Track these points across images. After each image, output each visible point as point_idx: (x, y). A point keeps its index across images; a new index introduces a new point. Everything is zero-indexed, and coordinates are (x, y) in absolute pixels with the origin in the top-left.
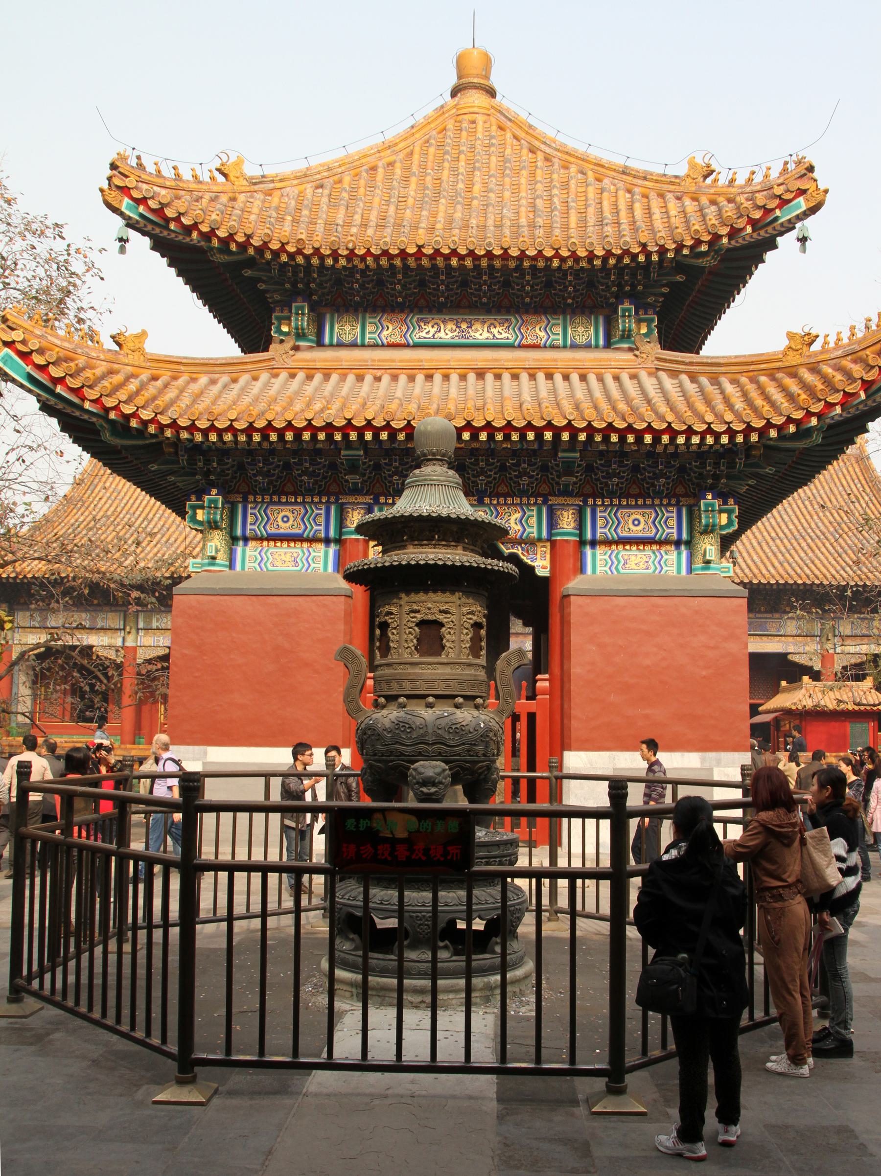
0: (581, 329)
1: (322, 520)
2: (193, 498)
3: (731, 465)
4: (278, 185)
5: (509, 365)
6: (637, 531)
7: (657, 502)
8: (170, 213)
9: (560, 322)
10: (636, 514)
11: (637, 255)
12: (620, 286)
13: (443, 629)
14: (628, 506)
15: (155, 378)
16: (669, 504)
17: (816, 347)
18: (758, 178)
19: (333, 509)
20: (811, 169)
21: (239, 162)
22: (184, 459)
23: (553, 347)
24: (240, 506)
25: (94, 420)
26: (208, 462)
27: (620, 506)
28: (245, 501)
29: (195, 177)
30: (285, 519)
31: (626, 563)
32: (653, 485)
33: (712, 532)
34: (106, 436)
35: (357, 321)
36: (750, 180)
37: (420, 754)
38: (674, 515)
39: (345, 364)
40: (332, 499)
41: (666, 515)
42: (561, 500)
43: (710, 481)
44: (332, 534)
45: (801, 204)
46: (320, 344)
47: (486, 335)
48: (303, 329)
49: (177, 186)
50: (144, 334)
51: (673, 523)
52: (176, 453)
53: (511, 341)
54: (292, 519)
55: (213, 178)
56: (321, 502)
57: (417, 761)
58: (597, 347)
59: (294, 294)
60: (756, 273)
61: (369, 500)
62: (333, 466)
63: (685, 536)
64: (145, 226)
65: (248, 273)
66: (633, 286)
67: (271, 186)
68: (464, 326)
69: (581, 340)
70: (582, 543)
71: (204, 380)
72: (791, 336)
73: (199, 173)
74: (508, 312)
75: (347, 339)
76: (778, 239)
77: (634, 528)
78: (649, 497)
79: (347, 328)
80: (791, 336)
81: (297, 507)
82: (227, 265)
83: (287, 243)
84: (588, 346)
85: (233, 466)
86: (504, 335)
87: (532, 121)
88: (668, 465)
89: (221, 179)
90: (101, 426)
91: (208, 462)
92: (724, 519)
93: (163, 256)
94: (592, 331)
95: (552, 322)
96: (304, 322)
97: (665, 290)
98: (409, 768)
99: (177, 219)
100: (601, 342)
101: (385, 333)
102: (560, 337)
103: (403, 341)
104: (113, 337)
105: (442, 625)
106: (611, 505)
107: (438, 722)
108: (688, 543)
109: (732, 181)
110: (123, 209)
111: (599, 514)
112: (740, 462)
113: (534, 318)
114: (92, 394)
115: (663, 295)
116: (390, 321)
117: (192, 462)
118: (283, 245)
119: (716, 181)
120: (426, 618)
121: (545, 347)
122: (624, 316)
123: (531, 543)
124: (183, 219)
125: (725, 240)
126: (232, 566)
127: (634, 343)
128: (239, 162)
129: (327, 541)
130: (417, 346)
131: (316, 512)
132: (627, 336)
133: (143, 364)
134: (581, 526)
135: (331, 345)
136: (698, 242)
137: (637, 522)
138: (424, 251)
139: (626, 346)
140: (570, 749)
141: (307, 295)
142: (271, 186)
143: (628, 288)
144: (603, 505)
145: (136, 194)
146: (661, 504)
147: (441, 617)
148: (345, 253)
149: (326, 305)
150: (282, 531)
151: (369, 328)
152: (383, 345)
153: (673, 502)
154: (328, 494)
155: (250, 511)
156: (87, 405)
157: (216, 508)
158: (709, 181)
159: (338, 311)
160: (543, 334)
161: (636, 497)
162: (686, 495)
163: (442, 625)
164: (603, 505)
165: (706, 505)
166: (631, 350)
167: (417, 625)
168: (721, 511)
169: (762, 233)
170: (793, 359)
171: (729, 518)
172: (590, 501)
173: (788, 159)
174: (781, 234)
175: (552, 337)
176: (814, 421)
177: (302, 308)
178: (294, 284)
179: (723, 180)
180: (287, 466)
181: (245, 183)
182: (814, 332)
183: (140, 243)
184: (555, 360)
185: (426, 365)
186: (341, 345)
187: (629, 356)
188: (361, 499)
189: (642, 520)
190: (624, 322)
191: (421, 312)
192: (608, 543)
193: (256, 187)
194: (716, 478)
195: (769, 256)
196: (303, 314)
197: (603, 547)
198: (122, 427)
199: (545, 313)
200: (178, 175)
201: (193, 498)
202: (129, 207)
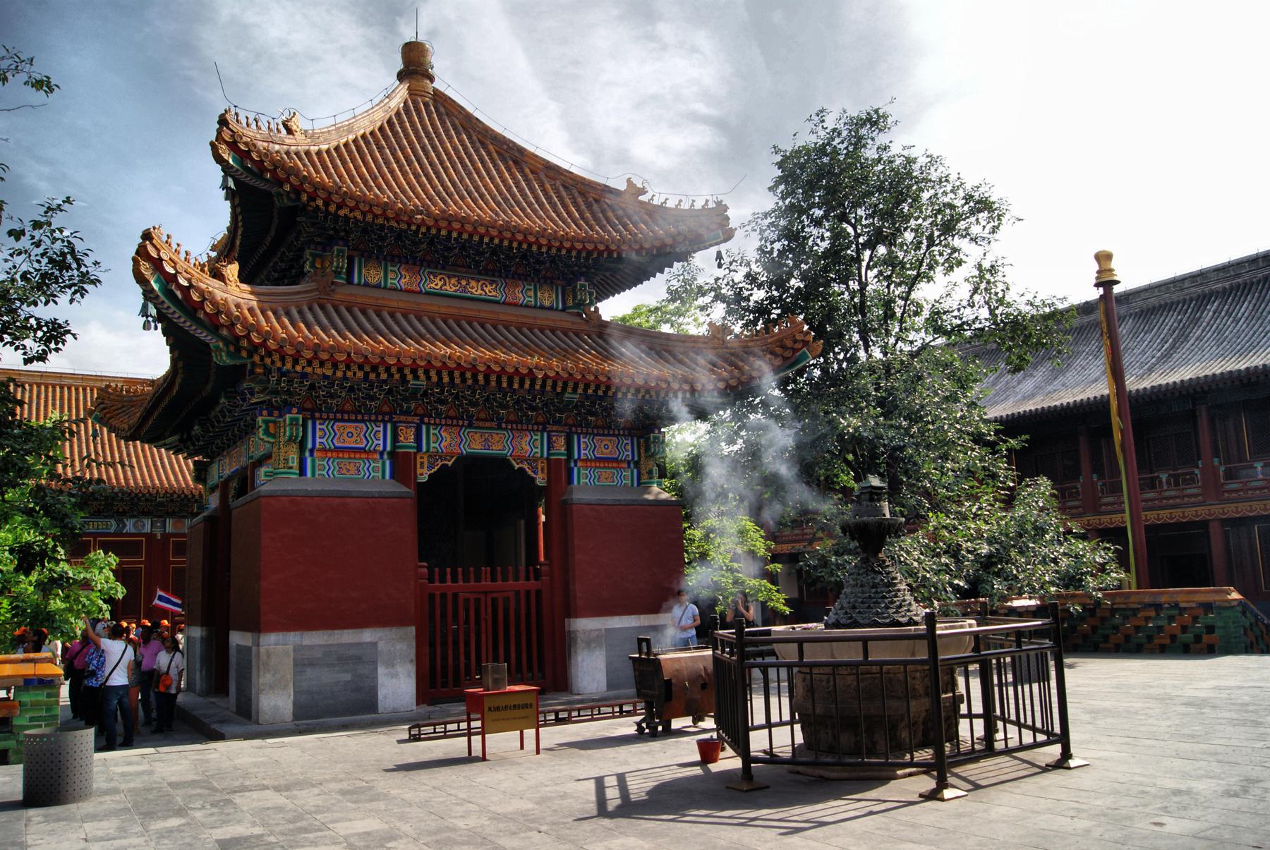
1: (381, 435)
2: (265, 413)
19: (389, 426)
27: (598, 435)
42: (555, 428)
47: (480, 291)
51: (629, 447)
58: (557, 309)
61: (416, 420)
68: (464, 283)
79: (373, 272)
84: (551, 308)
123: (532, 461)
126: (302, 472)
130: (427, 293)
140: (576, 617)
155: (318, 426)
188: (410, 419)
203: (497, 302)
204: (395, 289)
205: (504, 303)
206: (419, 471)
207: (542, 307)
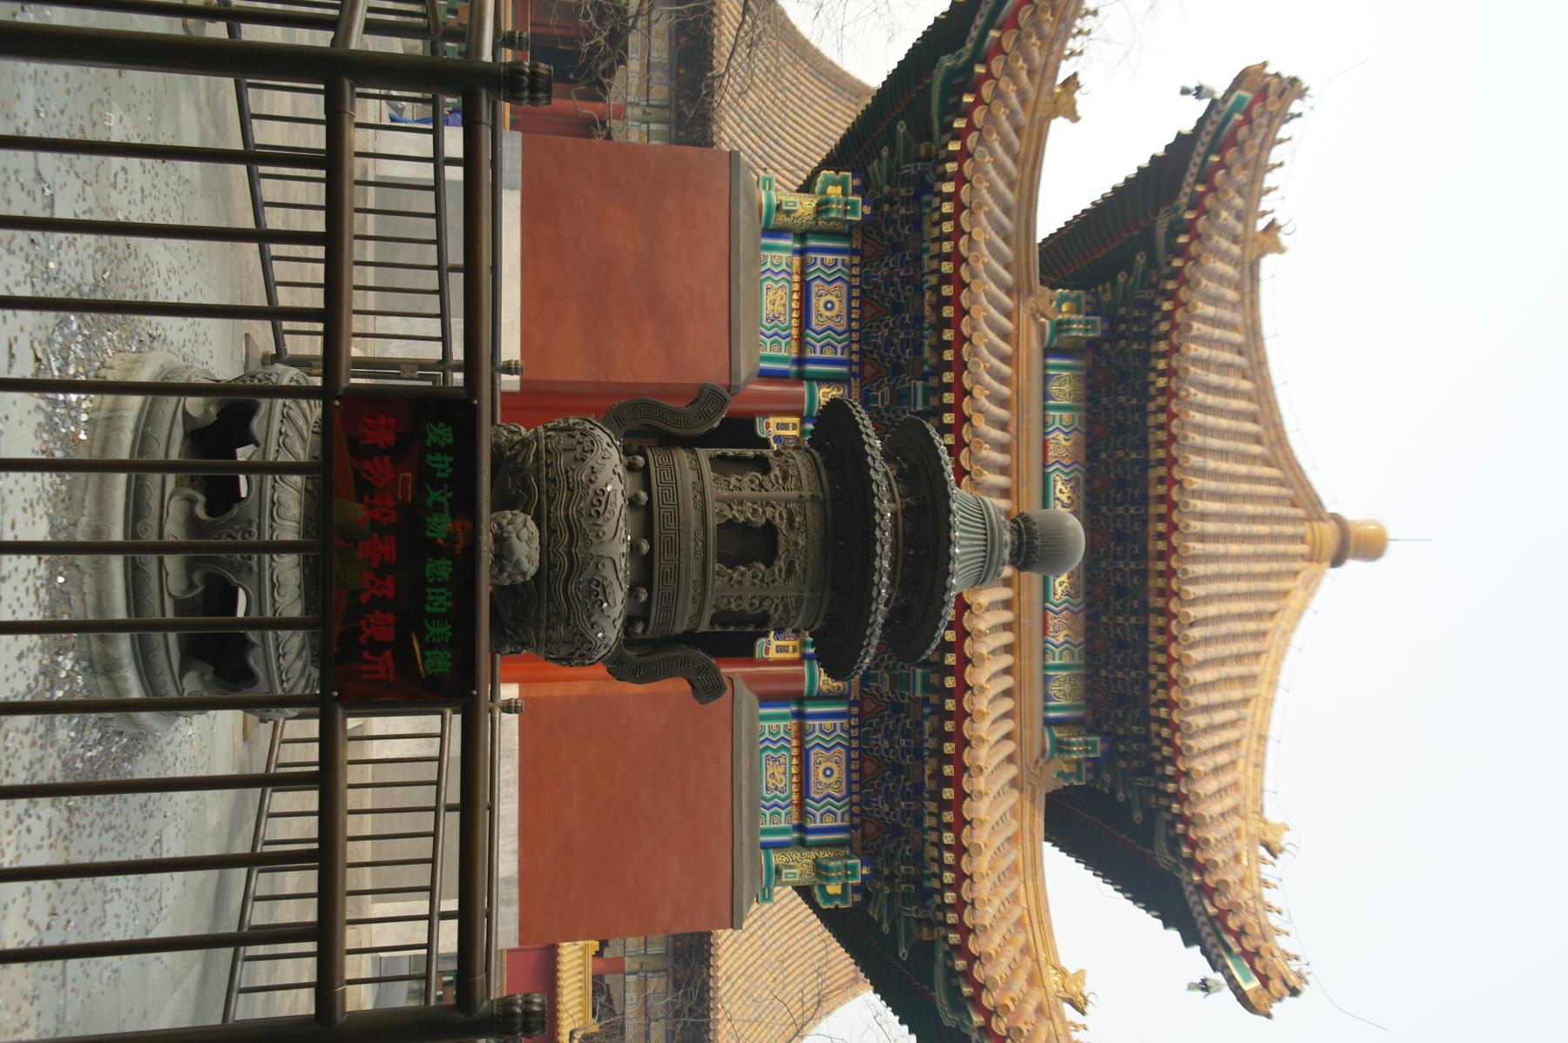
0: (1067, 688)
1: (828, 355)
2: (857, 182)
3: (908, 899)
4: (1247, 299)
5: (1024, 598)
6: (817, 774)
7: (856, 798)
8: (1231, 154)
9: (1077, 661)
10: (839, 772)
11: (1174, 765)
12: (1123, 739)
13: (762, 566)
14: (849, 760)
15: (1018, 131)
16: (852, 815)
17: (1070, 1013)
18: (1273, 919)
20: (1294, 992)
21: (1279, 249)
22: (910, 169)
23: (1045, 652)
24: (845, 245)
25: (969, 45)
26: (906, 201)
27: (849, 749)
28: (852, 252)
29: (1269, 190)
30: (829, 306)
31: (775, 760)
32: (877, 793)
33: (818, 874)
34: (947, 62)
35: (1075, 400)
36: (1269, 908)
37: (551, 531)
38: (839, 823)
39: (1023, 382)
40: (855, 369)
41: (839, 812)
43: (886, 871)
44: (811, 368)
45: (1251, 985)
46: (1048, 352)
48: (1068, 330)
49: (1260, 167)
50: (1074, 117)
51: (829, 822)
52: (917, 159)
53: (1051, 598)
54: (829, 314)
55: (1264, 214)
56: (852, 353)
57: (539, 526)
58: (1046, 709)
59: (1111, 318)
60: (1149, 917)
62: (898, 369)
63: (811, 838)
64: (1213, 123)
65: (1140, 259)
66: (1124, 755)
67: (1247, 289)
69: (1054, 689)
70: (800, 699)
71: (1010, 197)
72: (1080, 975)
73: (1271, 195)
74: (1088, 594)
75: (1053, 388)
76: (1197, 949)
77: (820, 771)
78: (862, 787)
79: (1067, 388)
80: (1080, 975)
81: (844, 321)
82: (1150, 233)
83: (1187, 311)
84: (1047, 697)
85: (899, 236)
86: (1059, 590)
87: (1308, 615)
88: (906, 813)
89: (1261, 224)
90: (959, 56)
91: (906, 201)
92: (834, 889)
93: (1168, 148)
94: (1063, 702)
95: (1076, 651)
96: (1077, 330)
97: (1121, 797)
98: (525, 511)
99: (1221, 165)
100: (1052, 714)
101: (1061, 436)
102: (1057, 662)
103: (1051, 460)
104: (1075, 75)
105: (769, 564)
106: (851, 738)
107: (608, 563)
108: (802, 843)
109: (1265, 884)
110: (1240, 93)
111: (838, 722)
112: (912, 910)
113: (1080, 625)
114: (1008, 43)
115: (1113, 792)
116: (1076, 443)
117: (906, 180)
118: (1184, 304)
119: (1264, 861)
120: (781, 538)
121: (1045, 642)
122: (1087, 743)
124: (1221, 172)
125: (1196, 878)
127: (1052, 756)
128: (1279, 249)
129: (800, 361)
130: (1045, 478)
131: (839, 347)
132: (1061, 747)
133: (1038, 116)
134: (823, 698)
135: (1045, 367)
136: (1194, 845)
137: (828, 773)
138: (1175, 489)
139: (1048, 746)
141: (1111, 336)
142: (1247, 289)
143: (1122, 748)
144: (851, 727)
145: (1257, 109)
146: (852, 804)
147: (781, 563)
148: (1173, 386)
149: (1094, 361)
150: (814, 300)
151: (1066, 415)
152: (1045, 434)
153: (856, 820)
154: (861, 364)
155: (840, 258)
156: (994, 34)
157: (846, 212)
158: (1263, 851)
159: (1089, 375)
160: (1061, 639)
161: (861, 771)
162: (864, 836)
163: (769, 564)
164: (851, 727)
165: (853, 868)
166: (1044, 751)
167: (768, 521)
168: (844, 886)
169: (1207, 929)
170: (1052, 978)
171: (835, 896)
172: (855, 710)
173: (1303, 960)
174: (1204, 952)
175: (1057, 651)
176: (978, 1019)
177: (1094, 329)
178: (1123, 319)
179: (1267, 871)
180: (897, 309)
181: (1254, 255)
182: (1088, 1009)
183: (1188, 115)
184: (1030, 657)
185: (1023, 491)
186: (1046, 379)
187: (1037, 752)
189: (832, 780)
190: (1079, 744)
191: (1088, 482)
192: (801, 734)
193: (1247, 271)
194: (890, 879)
195: (1174, 935)
196: (1087, 330)
197: (794, 728)
198: (963, 80)
199: (1088, 641)
200: (1274, 166)
201: (857, 182)
202: (1240, 100)
203: (1045, 598)
204: (1045, 424)
205: (1045, 609)
206: (773, 421)
207: (1046, 680)
